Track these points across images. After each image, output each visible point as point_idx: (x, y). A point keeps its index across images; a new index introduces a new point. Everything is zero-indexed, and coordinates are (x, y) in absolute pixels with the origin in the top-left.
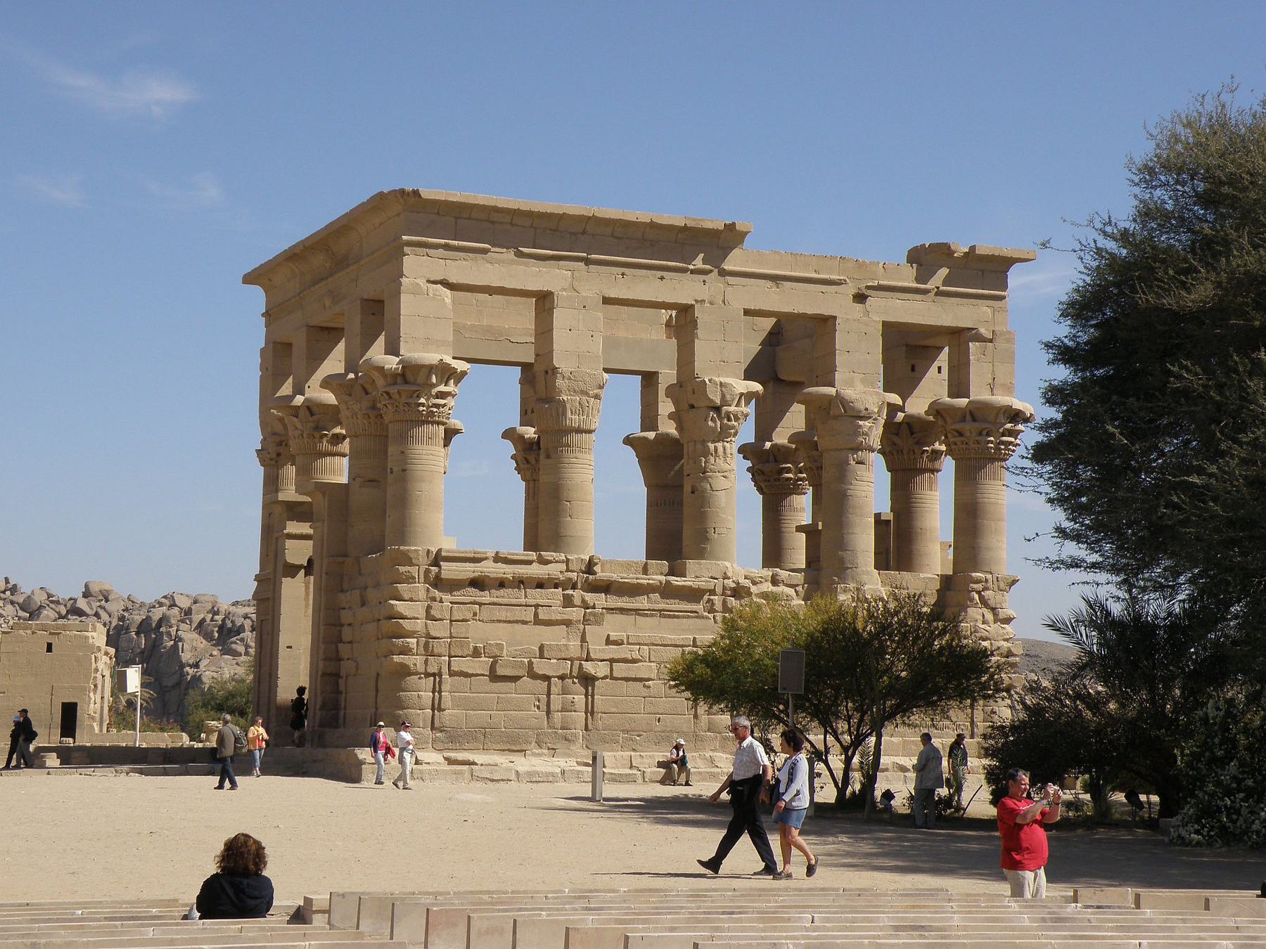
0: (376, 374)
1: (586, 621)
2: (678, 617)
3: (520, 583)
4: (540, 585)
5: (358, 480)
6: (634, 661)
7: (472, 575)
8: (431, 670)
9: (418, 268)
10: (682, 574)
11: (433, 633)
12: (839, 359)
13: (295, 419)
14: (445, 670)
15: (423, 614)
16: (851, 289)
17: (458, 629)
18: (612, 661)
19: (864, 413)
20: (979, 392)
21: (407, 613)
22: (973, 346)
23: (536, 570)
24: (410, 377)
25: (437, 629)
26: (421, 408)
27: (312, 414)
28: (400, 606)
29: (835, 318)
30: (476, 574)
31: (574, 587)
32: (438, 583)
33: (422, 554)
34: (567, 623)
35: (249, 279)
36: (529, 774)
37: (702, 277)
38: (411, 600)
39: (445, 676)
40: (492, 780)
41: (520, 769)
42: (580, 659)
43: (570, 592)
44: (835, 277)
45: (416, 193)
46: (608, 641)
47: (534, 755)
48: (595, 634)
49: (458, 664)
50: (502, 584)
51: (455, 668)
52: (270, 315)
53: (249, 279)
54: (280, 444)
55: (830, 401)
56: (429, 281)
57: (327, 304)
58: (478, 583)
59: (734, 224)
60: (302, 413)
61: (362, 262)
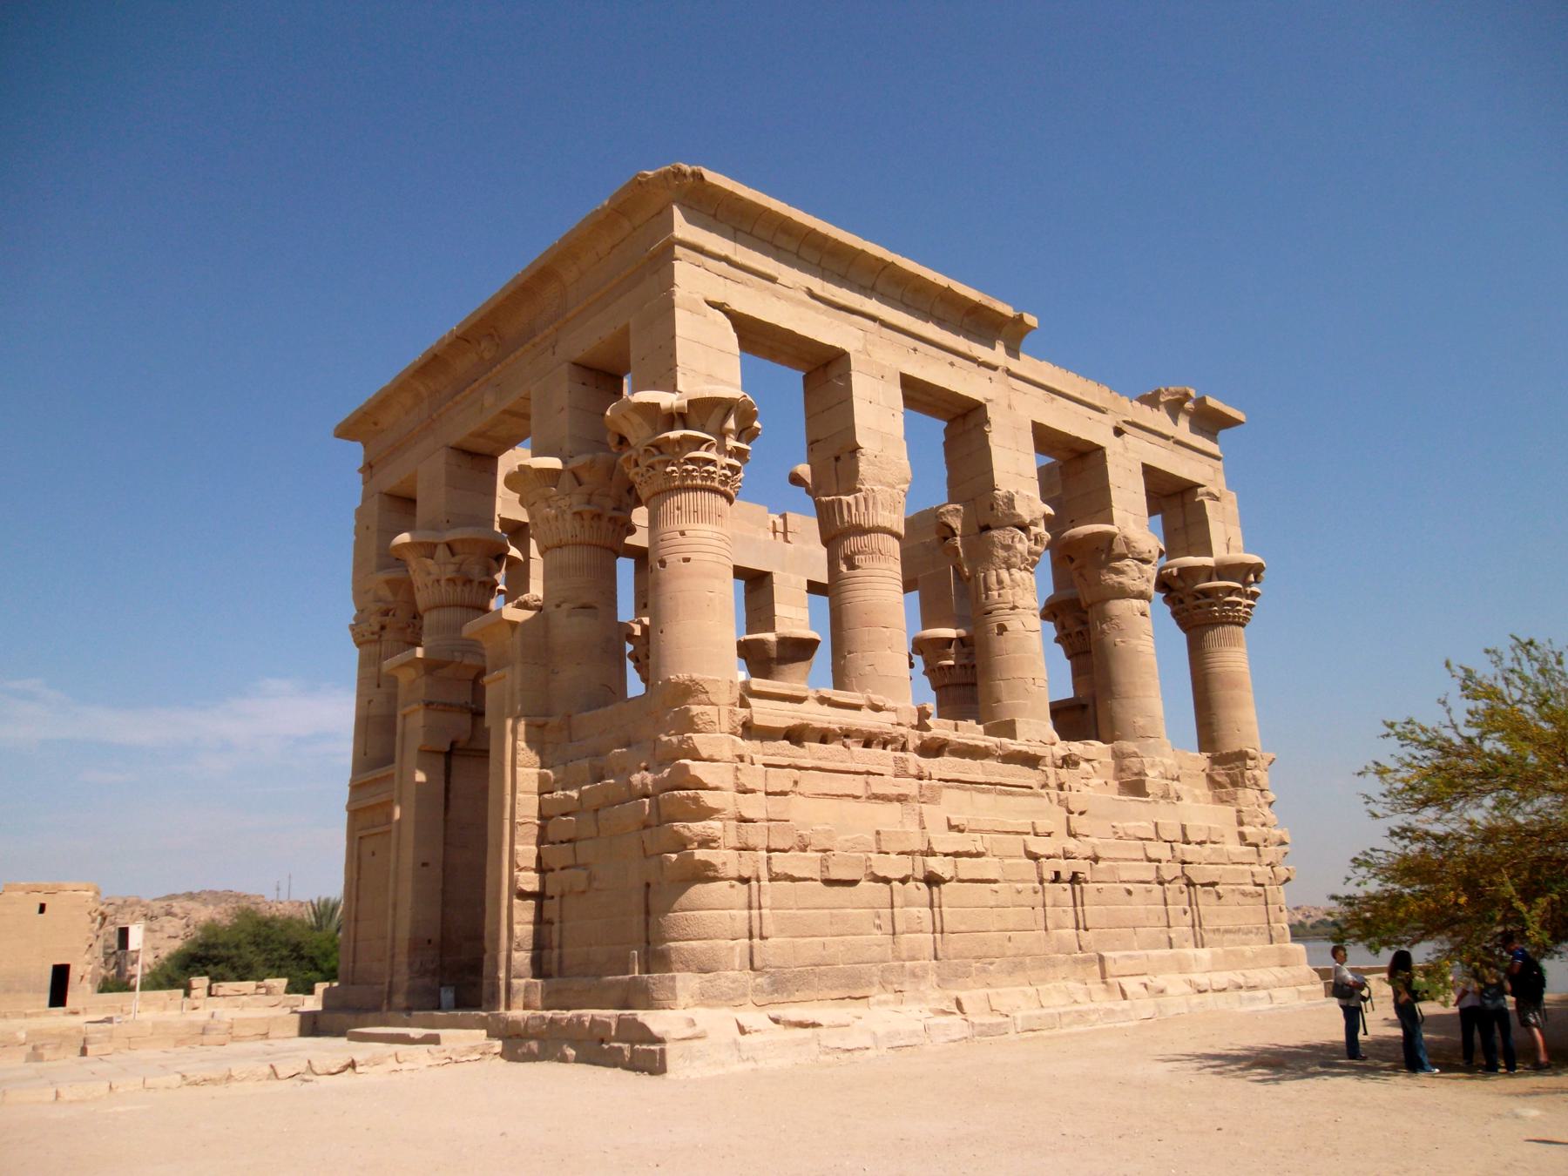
0: (636, 419)
1: (923, 798)
2: (1011, 794)
4: (867, 744)
5: (565, 606)
6: (979, 855)
8: (746, 874)
9: (692, 281)
11: (747, 815)
12: (1114, 494)
13: (429, 562)
14: (764, 874)
16: (1109, 421)
18: (957, 855)
19: (1145, 556)
21: (708, 779)
22: (1208, 504)
23: (865, 720)
24: (693, 418)
25: (753, 806)
26: (711, 468)
27: (453, 554)
28: (697, 769)
29: (1100, 449)
31: (904, 748)
32: (750, 730)
33: (725, 687)
34: (901, 799)
35: (346, 431)
38: (712, 760)
39: (765, 883)
41: (880, 1030)
42: (923, 854)
44: (1097, 403)
46: (951, 827)
47: (879, 1003)
48: (935, 814)
49: (781, 863)
50: (824, 737)
51: (776, 869)
52: (369, 468)
53: (346, 431)
54: (386, 613)
55: (1110, 537)
56: (708, 303)
57: (489, 399)
58: (796, 735)
59: (1021, 317)
60: (442, 552)
61: (569, 315)
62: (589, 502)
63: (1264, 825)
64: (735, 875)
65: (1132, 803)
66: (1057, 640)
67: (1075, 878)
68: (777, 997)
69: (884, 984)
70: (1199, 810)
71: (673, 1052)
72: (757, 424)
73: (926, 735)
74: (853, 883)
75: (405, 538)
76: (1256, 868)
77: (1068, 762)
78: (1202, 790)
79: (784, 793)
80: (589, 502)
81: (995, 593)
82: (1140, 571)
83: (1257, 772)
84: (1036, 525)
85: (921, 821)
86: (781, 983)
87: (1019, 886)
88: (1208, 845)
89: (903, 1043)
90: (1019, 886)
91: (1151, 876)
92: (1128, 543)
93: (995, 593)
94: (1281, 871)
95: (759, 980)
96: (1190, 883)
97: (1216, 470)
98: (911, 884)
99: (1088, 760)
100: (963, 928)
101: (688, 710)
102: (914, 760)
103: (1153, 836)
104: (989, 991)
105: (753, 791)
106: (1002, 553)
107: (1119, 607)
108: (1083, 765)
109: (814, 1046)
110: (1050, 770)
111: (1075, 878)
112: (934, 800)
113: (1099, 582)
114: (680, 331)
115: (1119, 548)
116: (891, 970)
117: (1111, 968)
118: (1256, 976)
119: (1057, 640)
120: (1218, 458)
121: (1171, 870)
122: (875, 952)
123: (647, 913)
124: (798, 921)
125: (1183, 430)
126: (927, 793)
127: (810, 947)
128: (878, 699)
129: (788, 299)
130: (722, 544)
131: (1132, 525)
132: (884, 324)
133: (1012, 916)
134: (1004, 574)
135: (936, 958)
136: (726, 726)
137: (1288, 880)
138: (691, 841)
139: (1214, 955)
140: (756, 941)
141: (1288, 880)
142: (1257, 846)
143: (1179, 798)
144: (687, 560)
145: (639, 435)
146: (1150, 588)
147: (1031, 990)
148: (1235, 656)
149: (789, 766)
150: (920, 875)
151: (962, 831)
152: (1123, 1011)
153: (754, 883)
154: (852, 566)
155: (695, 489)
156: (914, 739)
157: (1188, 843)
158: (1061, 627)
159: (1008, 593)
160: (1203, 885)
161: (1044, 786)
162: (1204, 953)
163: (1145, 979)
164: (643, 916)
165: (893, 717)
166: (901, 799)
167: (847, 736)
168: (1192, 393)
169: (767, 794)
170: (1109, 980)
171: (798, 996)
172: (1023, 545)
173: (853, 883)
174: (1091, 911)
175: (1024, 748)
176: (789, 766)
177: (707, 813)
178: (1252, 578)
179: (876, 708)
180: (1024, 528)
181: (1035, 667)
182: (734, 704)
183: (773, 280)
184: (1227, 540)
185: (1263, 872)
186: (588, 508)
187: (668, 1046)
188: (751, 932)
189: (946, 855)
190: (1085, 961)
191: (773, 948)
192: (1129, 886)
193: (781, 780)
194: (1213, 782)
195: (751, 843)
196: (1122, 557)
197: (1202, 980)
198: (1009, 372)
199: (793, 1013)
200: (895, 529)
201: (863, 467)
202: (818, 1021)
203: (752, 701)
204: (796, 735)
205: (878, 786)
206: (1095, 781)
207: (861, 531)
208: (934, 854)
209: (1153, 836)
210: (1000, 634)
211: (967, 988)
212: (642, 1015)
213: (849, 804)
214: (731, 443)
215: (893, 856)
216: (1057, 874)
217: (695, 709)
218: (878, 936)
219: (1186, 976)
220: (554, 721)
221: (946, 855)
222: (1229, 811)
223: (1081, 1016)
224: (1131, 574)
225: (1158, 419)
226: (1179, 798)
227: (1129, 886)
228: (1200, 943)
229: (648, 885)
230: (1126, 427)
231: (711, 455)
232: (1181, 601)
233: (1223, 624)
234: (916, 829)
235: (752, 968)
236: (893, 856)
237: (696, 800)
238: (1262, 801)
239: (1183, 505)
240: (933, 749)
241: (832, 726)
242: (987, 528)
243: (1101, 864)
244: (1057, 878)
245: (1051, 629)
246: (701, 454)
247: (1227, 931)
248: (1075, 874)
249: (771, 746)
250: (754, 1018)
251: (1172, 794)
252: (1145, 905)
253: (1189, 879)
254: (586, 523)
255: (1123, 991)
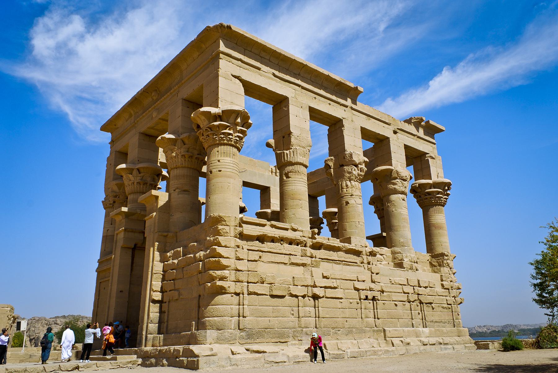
0: (203, 118)
3: (281, 240)
4: (290, 244)
6: (335, 288)
7: (259, 234)
8: (238, 291)
9: (226, 67)
10: (350, 243)
11: (239, 268)
14: (245, 292)
15: (233, 255)
16: (392, 128)
17: (252, 265)
18: (326, 287)
19: (404, 178)
20: (435, 179)
22: (430, 160)
23: (289, 234)
24: (224, 117)
25: (241, 265)
26: (231, 137)
28: (219, 250)
29: (388, 138)
30: (261, 233)
31: (305, 246)
32: (242, 236)
33: (233, 219)
34: (304, 265)
36: (295, 357)
37: (345, 108)
38: (226, 247)
39: (246, 295)
40: (277, 363)
42: (311, 286)
43: (304, 248)
44: (387, 121)
45: (229, 27)
46: (324, 277)
47: (292, 344)
48: (318, 272)
50: (273, 240)
51: (251, 290)
55: (391, 171)
58: (261, 239)
62: (188, 152)
63: (451, 281)
64: (234, 292)
65: (398, 271)
66: (375, 212)
67: (374, 299)
68: (249, 341)
69: (294, 337)
70: (426, 275)
71: (202, 361)
72: (250, 121)
73: (314, 240)
74: (283, 297)
75: (123, 166)
76: (448, 298)
77: (372, 254)
78: (428, 267)
79: (256, 261)
80: (188, 152)
81: (345, 190)
82: (402, 184)
83: (448, 261)
84: (361, 165)
85: (312, 274)
86: (251, 335)
87: (351, 301)
88: (429, 288)
89: (300, 360)
90: (351, 301)
91: (405, 299)
92: (397, 173)
93: (345, 190)
94: (458, 299)
95: (241, 334)
96: (421, 303)
97: (434, 148)
98: (307, 298)
99: (381, 255)
100: (327, 316)
101: (218, 227)
102: (309, 251)
103: (406, 283)
104: (337, 341)
105: (242, 259)
106: (348, 175)
107: (394, 197)
108: (378, 256)
109: (263, 361)
110: (365, 257)
111: (374, 299)
112: (317, 266)
113: (387, 188)
114: (220, 85)
115: (394, 175)
116: (298, 332)
117: (388, 334)
118: (447, 340)
119: (375, 212)
120: (435, 144)
121: (413, 297)
122: (291, 324)
123: (199, 307)
124: (259, 312)
125: (421, 133)
126: (314, 263)
127: (264, 322)
128: (295, 227)
129: (265, 76)
130: (235, 166)
131: (399, 166)
132: (303, 88)
133: (348, 312)
134: (348, 183)
135: (316, 328)
136: (232, 234)
137: (461, 303)
138: (216, 278)
139: (430, 331)
140: (241, 318)
141: (461, 303)
142: (448, 289)
143: (417, 270)
144: (220, 171)
145: (203, 123)
146: (407, 190)
147: (355, 342)
148: (440, 217)
149: (258, 251)
150: (310, 295)
151: (328, 278)
152: (392, 351)
153: (241, 295)
154: (288, 177)
155: (225, 144)
156: (310, 242)
157: (421, 287)
158: (376, 207)
159: (350, 190)
160: (426, 303)
161: (362, 263)
162: (426, 330)
163: (402, 339)
164: (197, 308)
165: (300, 234)
166: (304, 265)
167: (282, 240)
168: (424, 119)
169: (248, 261)
170: (387, 339)
171: (258, 341)
172: (356, 172)
173: (283, 297)
174: (381, 312)
175: (354, 248)
176: (258, 251)
177: (224, 268)
178: (446, 188)
179: (294, 230)
180: (356, 166)
181: (362, 221)
182: (236, 226)
183: (259, 69)
184: (437, 173)
185: (451, 300)
186: (187, 153)
187: (200, 359)
188: (239, 314)
189: (321, 287)
190: (377, 331)
191: (247, 322)
192: (396, 303)
193: (254, 256)
194: (432, 265)
195: (240, 279)
196: (396, 178)
197: (426, 340)
198: (352, 108)
199: (255, 347)
200: (305, 163)
201: (293, 140)
202: (265, 350)
203: (243, 225)
204: (261, 239)
205: (294, 260)
206: (384, 263)
207: (292, 164)
208: (316, 287)
209: (406, 283)
210: (346, 205)
211: (328, 340)
212: (191, 347)
213: (281, 265)
214: (239, 128)
215: (299, 287)
216: (367, 296)
217: (220, 227)
218: (292, 318)
219: (418, 338)
220: (170, 234)
221: (321, 287)
222: (438, 276)
223: (375, 353)
224: (399, 185)
225: (411, 128)
226: (417, 270)
227: (396, 303)
228: (425, 326)
229: (200, 296)
230: (398, 131)
231: (231, 132)
232: (420, 197)
233: (436, 205)
234: (310, 277)
235: (239, 329)
236: (299, 287)
237: (219, 261)
238: (451, 272)
239: (421, 161)
240: (317, 246)
241: (276, 236)
242: (342, 166)
243: (385, 294)
244: (367, 298)
245: (372, 208)
246: (227, 131)
247: (436, 322)
248: (374, 297)
249: (250, 243)
250: (237, 348)
251: (414, 268)
252: (402, 310)
253: (420, 301)
254: (187, 160)
255: (392, 343)
